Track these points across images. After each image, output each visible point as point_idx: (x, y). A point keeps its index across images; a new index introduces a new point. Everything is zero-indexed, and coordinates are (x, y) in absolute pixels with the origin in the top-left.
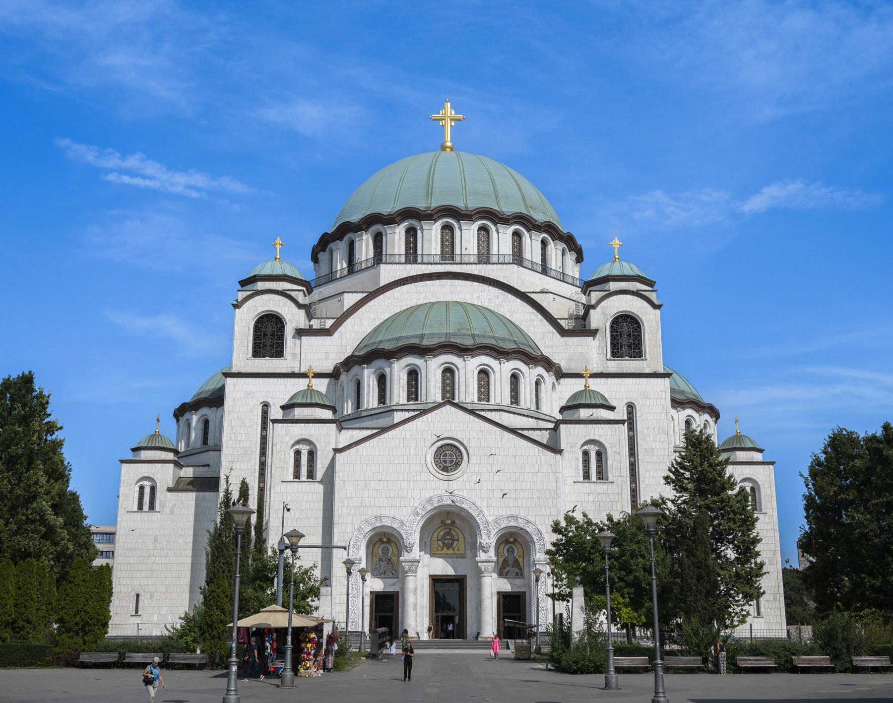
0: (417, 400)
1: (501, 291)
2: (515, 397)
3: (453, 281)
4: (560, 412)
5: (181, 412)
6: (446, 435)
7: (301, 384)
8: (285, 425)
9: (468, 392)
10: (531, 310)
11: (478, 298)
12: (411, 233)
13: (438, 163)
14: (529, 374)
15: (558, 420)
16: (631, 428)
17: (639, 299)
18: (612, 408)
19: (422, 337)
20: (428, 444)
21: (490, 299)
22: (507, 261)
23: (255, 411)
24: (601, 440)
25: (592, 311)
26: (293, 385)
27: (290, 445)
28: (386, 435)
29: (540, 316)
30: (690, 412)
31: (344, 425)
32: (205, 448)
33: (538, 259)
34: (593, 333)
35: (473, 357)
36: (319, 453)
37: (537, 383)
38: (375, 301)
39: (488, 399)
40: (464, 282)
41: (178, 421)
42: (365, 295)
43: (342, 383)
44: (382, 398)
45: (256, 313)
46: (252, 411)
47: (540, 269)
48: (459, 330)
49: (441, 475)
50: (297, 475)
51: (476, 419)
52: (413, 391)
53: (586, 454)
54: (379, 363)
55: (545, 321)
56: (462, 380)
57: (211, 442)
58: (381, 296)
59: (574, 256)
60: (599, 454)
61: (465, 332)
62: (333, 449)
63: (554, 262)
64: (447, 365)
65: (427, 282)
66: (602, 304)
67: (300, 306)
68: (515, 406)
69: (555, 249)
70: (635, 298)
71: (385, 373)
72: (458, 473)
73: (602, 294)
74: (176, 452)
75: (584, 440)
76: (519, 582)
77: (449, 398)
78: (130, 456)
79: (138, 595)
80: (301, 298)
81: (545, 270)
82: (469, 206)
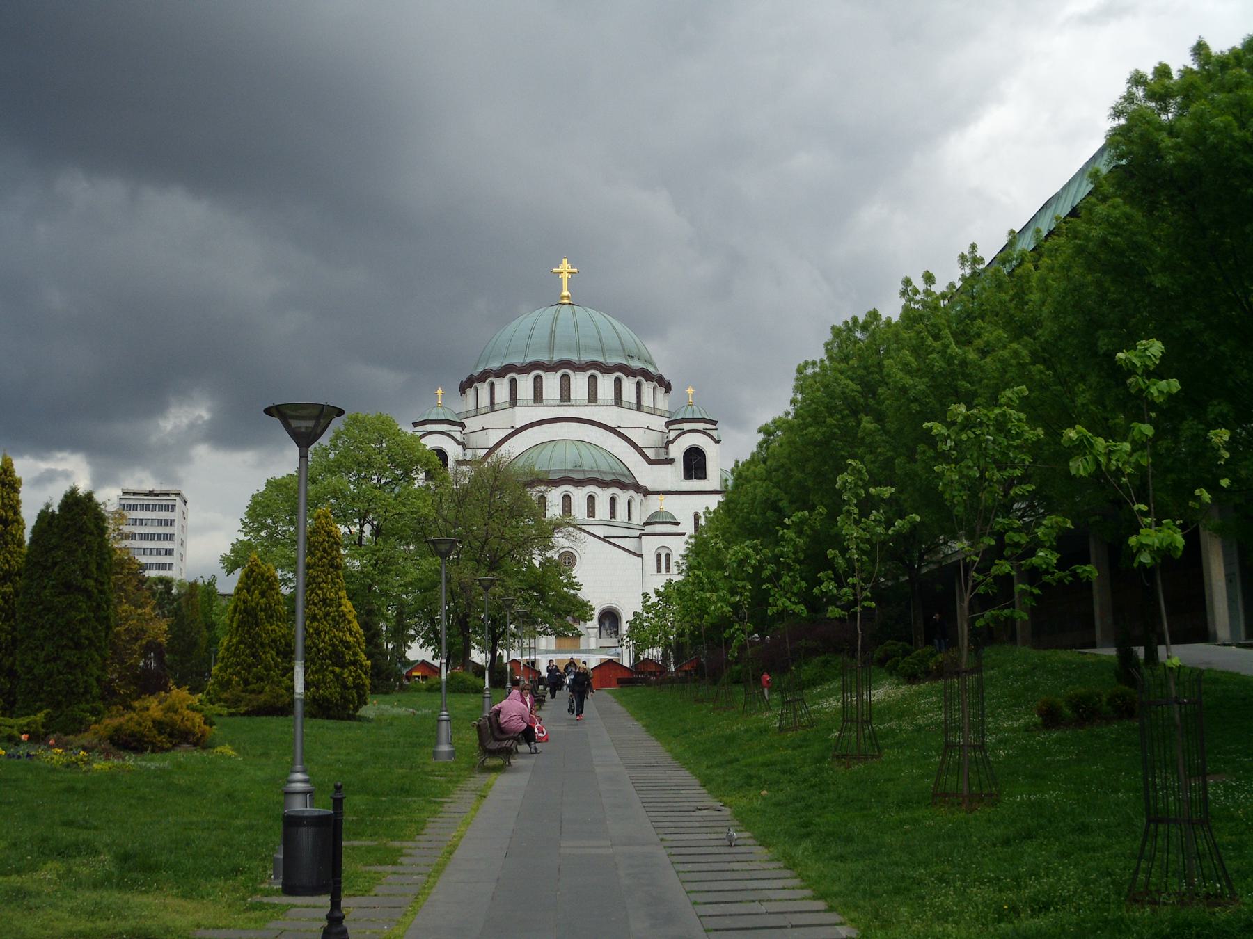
2: (613, 514)
12: (538, 381)
13: (558, 322)
14: (623, 497)
18: (678, 524)
19: (548, 472)
33: (634, 400)
47: (635, 407)
60: (668, 555)
61: (578, 468)
63: (647, 401)
67: (459, 443)
68: (613, 520)
69: (647, 388)
81: (639, 407)
82: (582, 359)
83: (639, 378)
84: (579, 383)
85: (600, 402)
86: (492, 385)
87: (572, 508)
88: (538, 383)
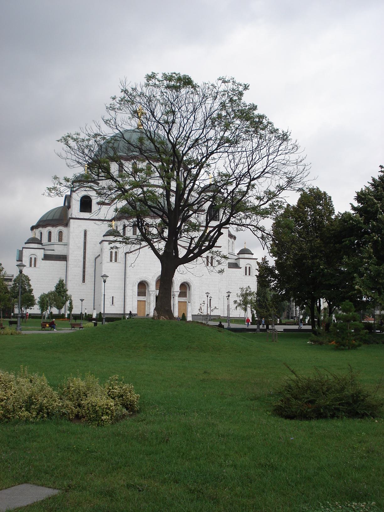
23: (82, 232)
32: (49, 243)
36: (119, 253)
46: (81, 233)
50: (111, 261)
57: (52, 241)
76: (185, 298)
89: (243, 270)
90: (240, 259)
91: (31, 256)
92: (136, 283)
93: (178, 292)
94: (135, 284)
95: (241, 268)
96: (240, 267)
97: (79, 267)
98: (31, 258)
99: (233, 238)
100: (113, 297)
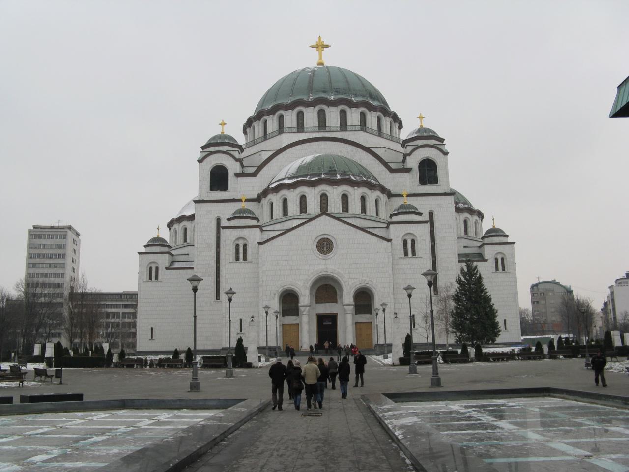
0: (306, 213)
1: (354, 147)
3: (326, 142)
4: (390, 217)
5: (170, 224)
6: (323, 233)
7: (238, 206)
8: (230, 230)
9: (335, 206)
10: (372, 158)
11: (341, 152)
14: (373, 196)
15: (389, 222)
16: (432, 225)
17: (435, 150)
18: (420, 214)
20: (313, 239)
21: (348, 152)
22: (357, 129)
24: (414, 233)
25: (408, 157)
26: (234, 206)
27: (233, 241)
28: (288, 234)
29: (377, 161)
30: (466, 215)
31: (264, 229)
33: (375, 127)
34: (409, 170)
35: (338, 186)
36: (250, 245)
37: (377, 201)
38: (280, 156)
39: (348, 212)
40: (332, 142)
41: (170, 229)
42: (274, 152)
43: (262, 204)
44: (285, 212)
45: (211, 165)
46: (211, 222)
47: (377, 133)
48: (329, 171)
49: (321, 256)
50: (237, 259)
51: (341, 223)
52: (303, 208)
53: (405, 242)
54: (284, 193)
55: (380, 164)
56: (332, 200)
57: (188, 241)
58: (284, 153)
59: (397, 125)
60: (413, 242)
62: (258, 243)
63: (386, 129)
64: (323, 192)
65: (311, 143)
66: (414, 153)
67: (237, 160)
68: (364, 214)
69: (386, 121)
70: (433, 149)
71: (286, 197)
72: (331, 255)
73: (413, 147)
74: (169, 247)
75: (403, 234)
76: (368, 316)
77: (324, 210)
78: (143, 250)
79: (152, 329)
80: (236, 155)
81: (380, 133)
83: (379, 113)
84: (333, 116)
85: (349, 128)
86: (266, 122)
87: (329, 204)
88: (300, 116)
89: (491, 262)
90: (485, 246)
91: (150, 265)
92: (275, 294)
93: (352, 305)
94: (273, 295)
95: (486, 260)
96: (486, 258)
97: (210, 276)
98: (151, 268)
99: (476, 213)
100: (241, 320)
